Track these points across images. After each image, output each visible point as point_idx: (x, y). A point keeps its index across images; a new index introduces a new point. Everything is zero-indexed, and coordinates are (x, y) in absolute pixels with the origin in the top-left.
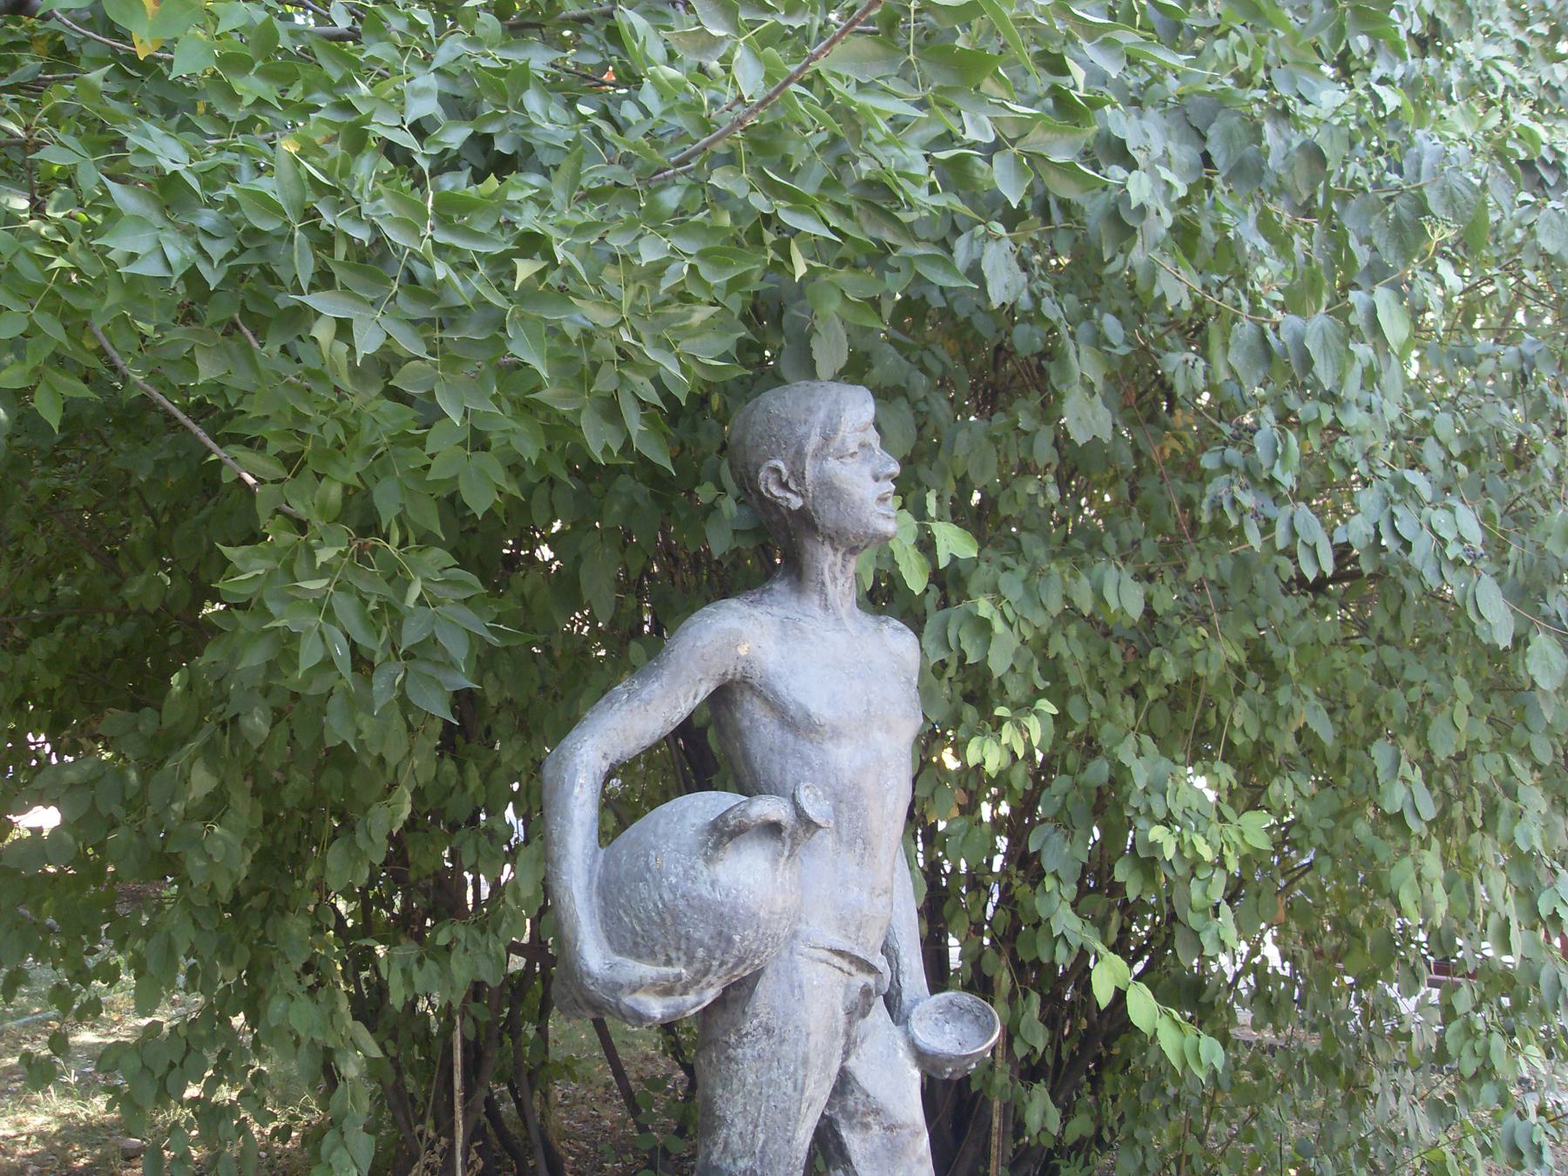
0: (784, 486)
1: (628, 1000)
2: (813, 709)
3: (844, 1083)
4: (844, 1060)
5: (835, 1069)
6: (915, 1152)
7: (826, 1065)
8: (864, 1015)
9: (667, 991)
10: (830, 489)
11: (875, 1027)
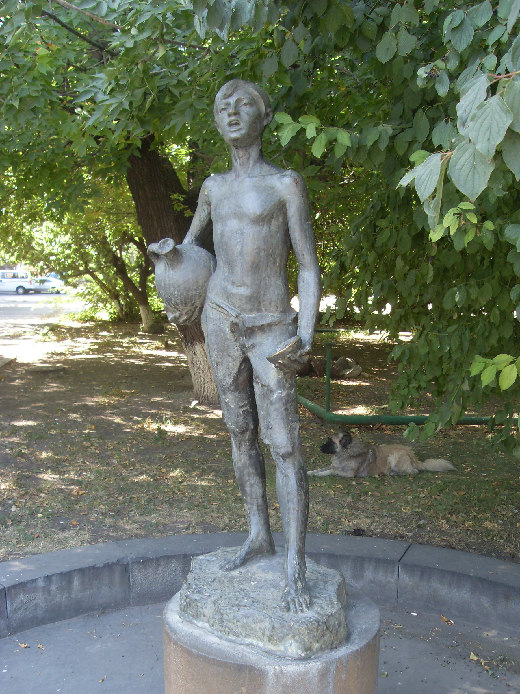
4: (243, 353)
5: (238, 354)
6: (269, 399)
11: (261, 344)
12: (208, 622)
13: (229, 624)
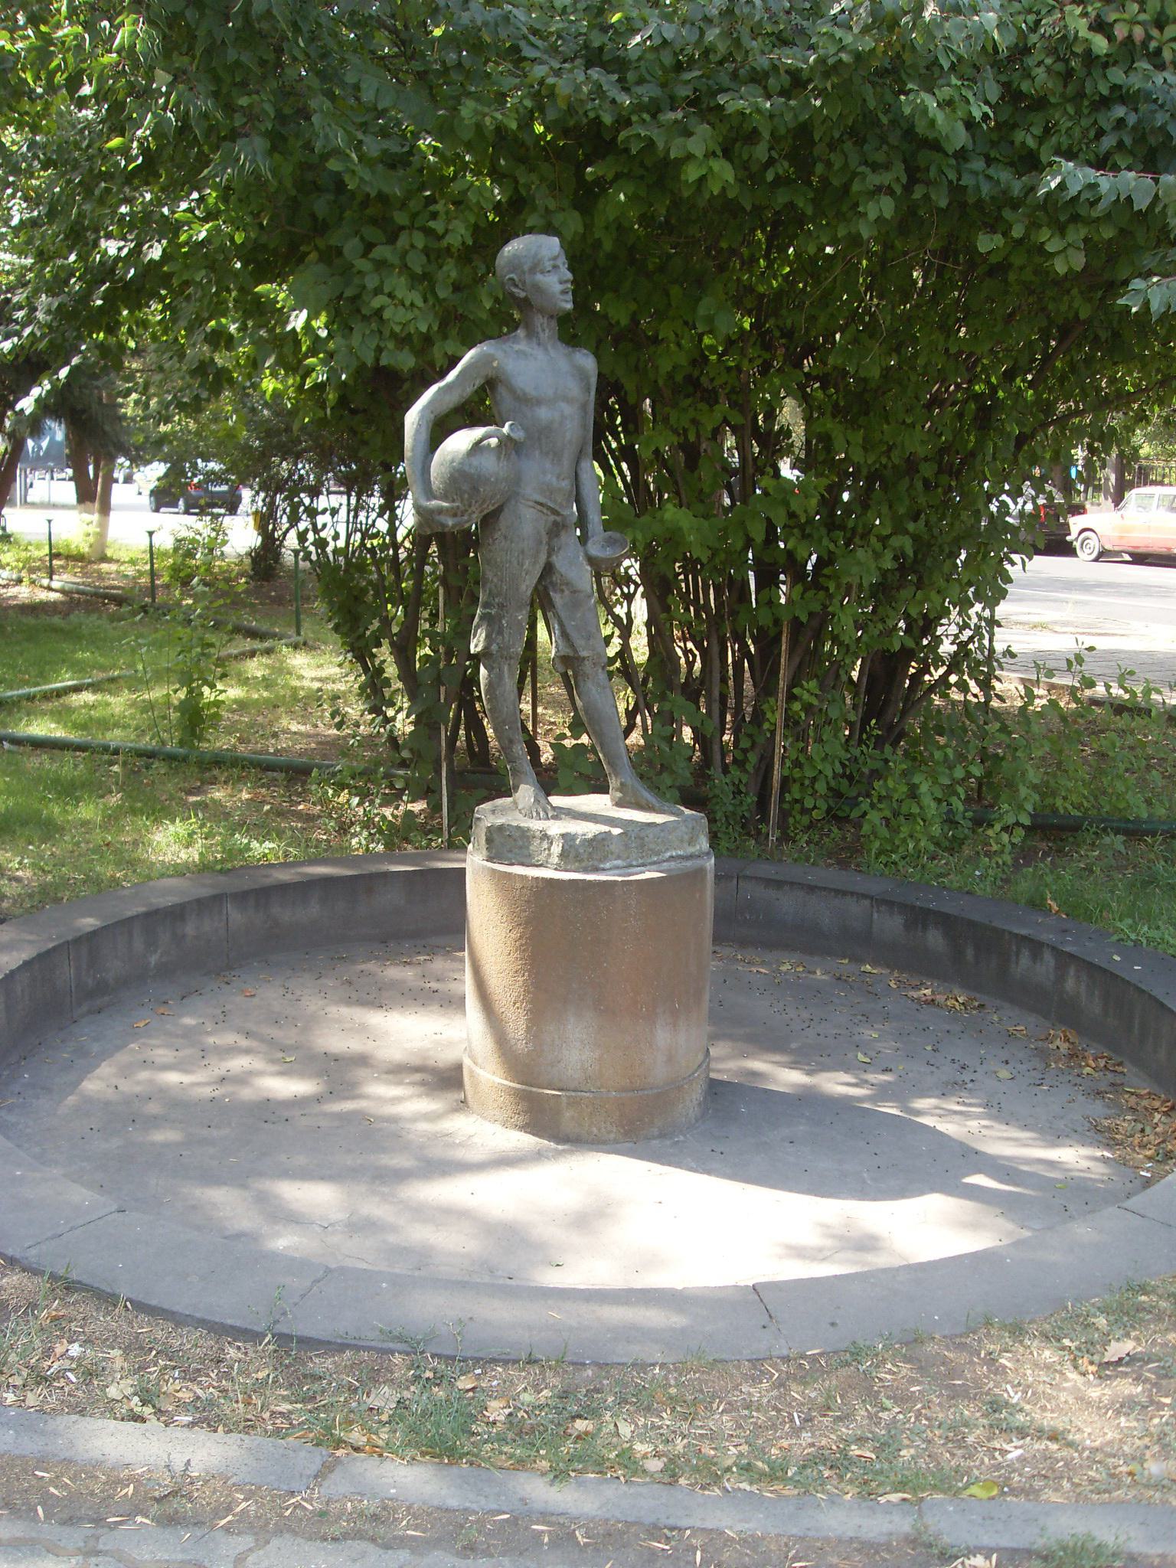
0: (516, 286)
1: (437, 517)
2: (527, 390)
3: (548, 569)
5: (543, 559)
7: (536, 556)
8: (557, 535)
9: (455, 515)
10: (538, 288)
12: (618, 858)
13: (652, 846)
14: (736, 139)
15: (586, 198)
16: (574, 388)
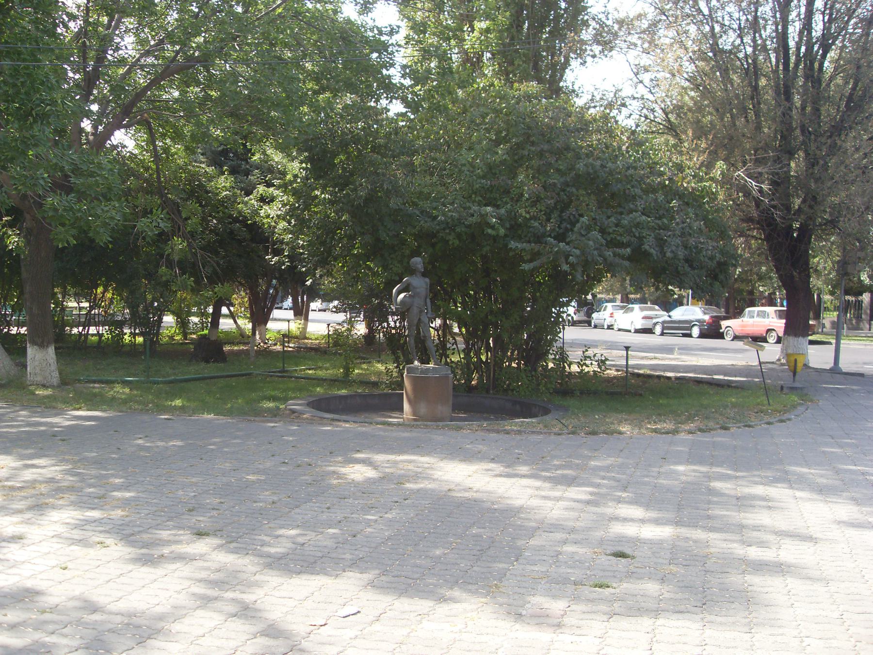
3: (420, 319)
14: (459, 236)
15: (433, 245)
16: (424, 286)
